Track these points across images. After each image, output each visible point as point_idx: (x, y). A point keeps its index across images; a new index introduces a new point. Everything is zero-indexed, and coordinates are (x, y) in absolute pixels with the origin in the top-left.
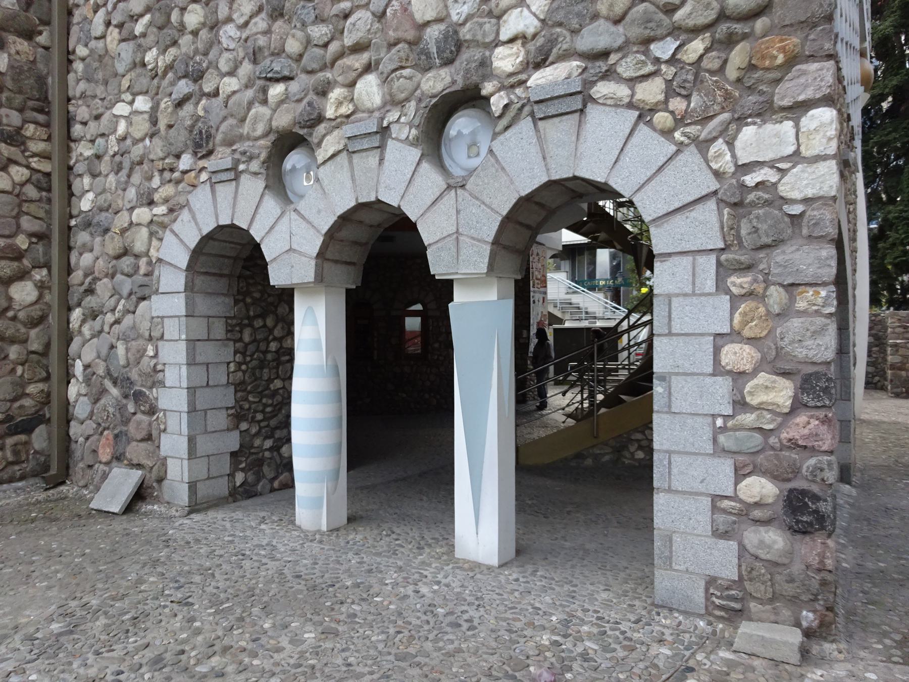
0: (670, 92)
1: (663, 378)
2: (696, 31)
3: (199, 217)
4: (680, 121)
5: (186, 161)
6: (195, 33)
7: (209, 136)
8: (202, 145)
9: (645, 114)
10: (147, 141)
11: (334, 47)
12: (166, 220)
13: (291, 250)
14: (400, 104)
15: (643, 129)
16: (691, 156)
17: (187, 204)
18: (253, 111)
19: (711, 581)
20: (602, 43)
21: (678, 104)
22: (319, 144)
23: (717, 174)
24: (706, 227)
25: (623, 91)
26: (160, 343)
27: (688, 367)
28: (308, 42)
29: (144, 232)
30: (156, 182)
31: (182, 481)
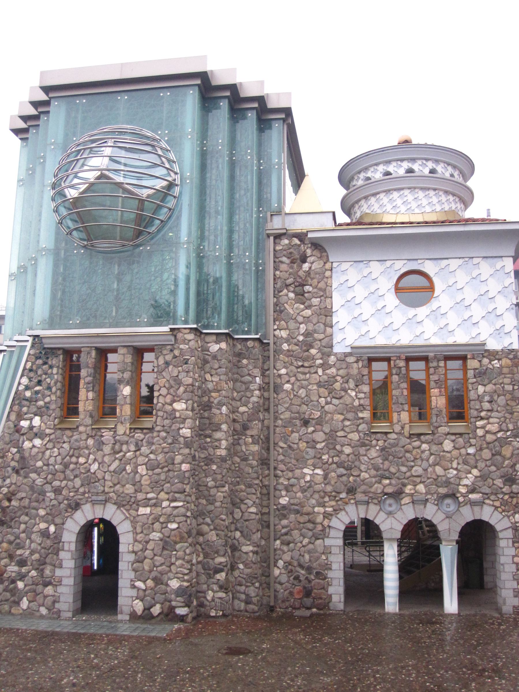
0: (501, 504)
1: (502, 565)
2: (506, 494)
3: (349, 513)
4: (504, 511)
5: (343, 495)
6: (348, 455)
7: (356, 489)
8: (351, 491)
9: (496, 508)
10: (323, 485)
11: (408, 474)
12: (333, 513)
13: (391, 528)
14: (432, 494)
15: (496, 512)
16: (506, 518)
17: (344, 509)
18: (376, 485)
19: (514, 607)
20: (487, 492)
21: (503, 507)
22: (402, 499)
23: (512, 523)
24: (509, 534)
25: (491, 503)
26: (329, 555)
27: (507, 562)
28: (399, 470)
29: (321, 516)
30: (327, 499)
31: (340, 602)
